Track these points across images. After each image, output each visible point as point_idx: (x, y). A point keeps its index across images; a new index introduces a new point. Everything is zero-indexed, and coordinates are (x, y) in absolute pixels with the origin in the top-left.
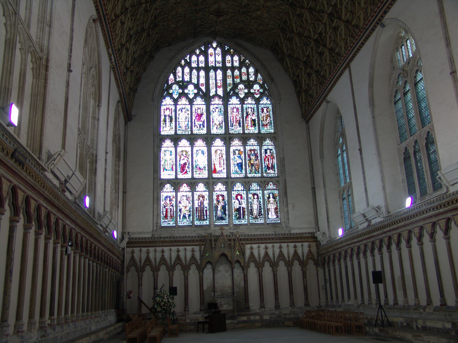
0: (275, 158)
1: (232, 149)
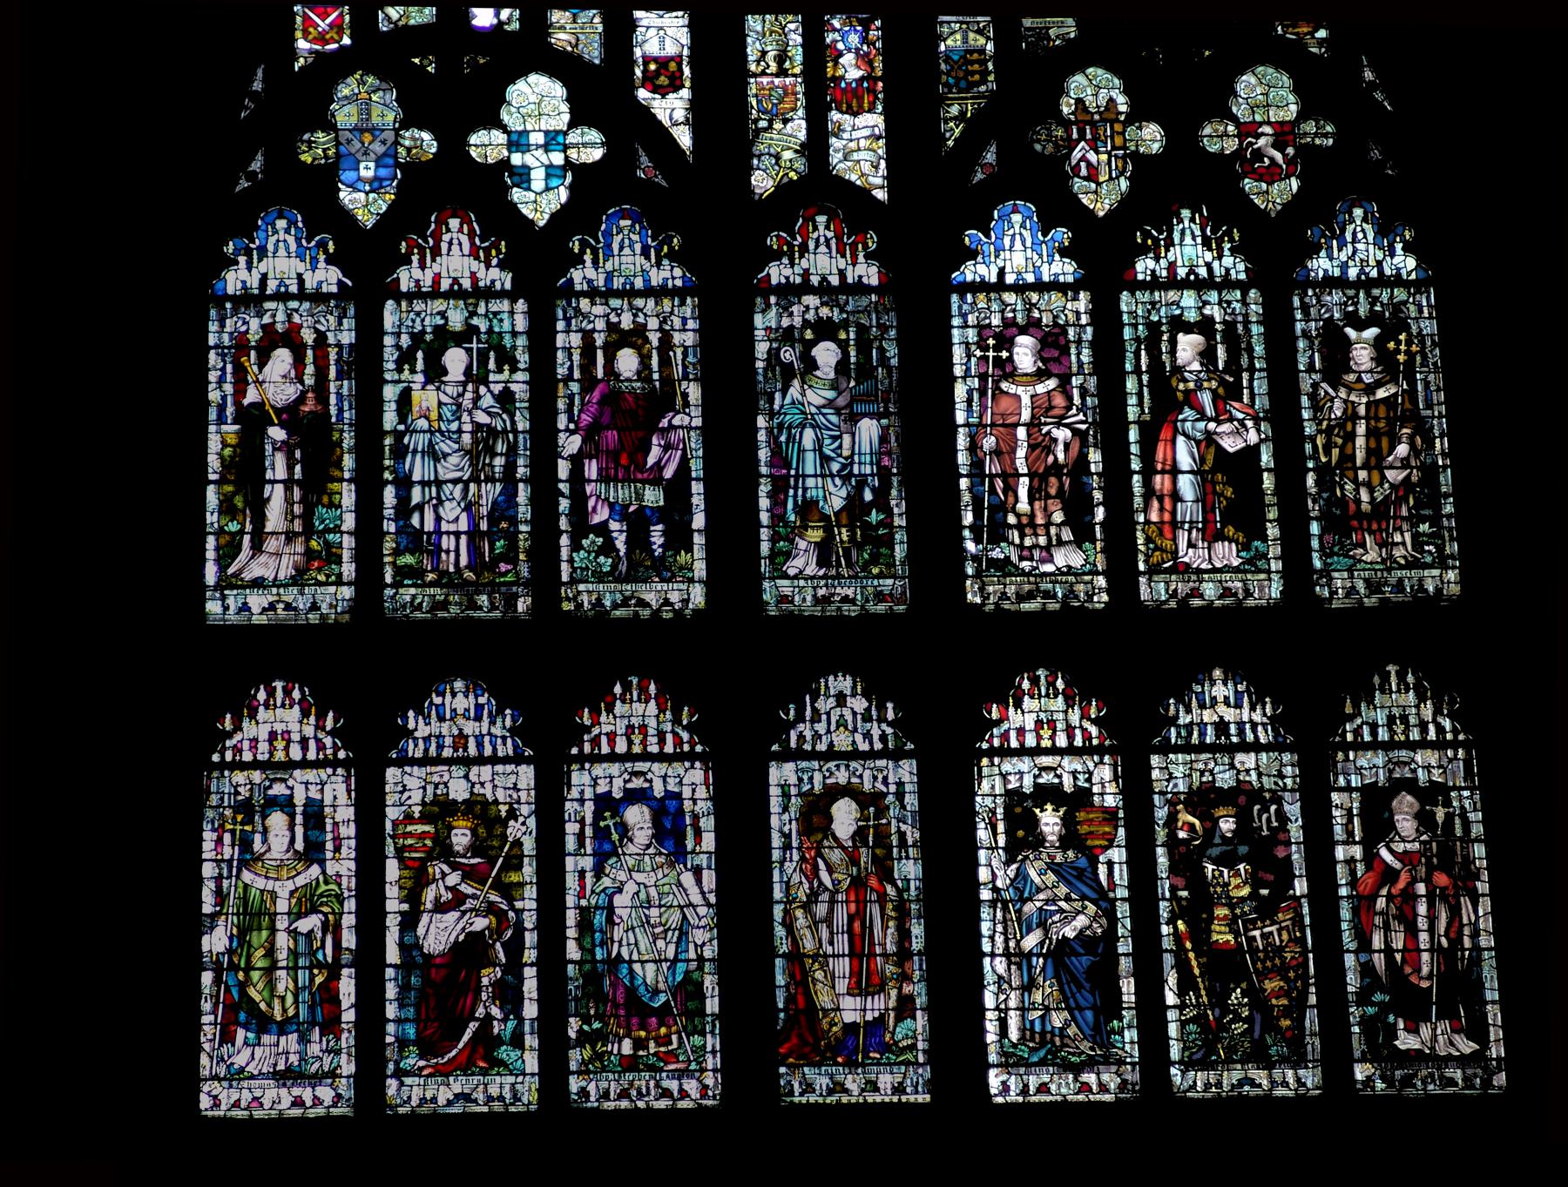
0: (1483, 887)
1: (989, 790)
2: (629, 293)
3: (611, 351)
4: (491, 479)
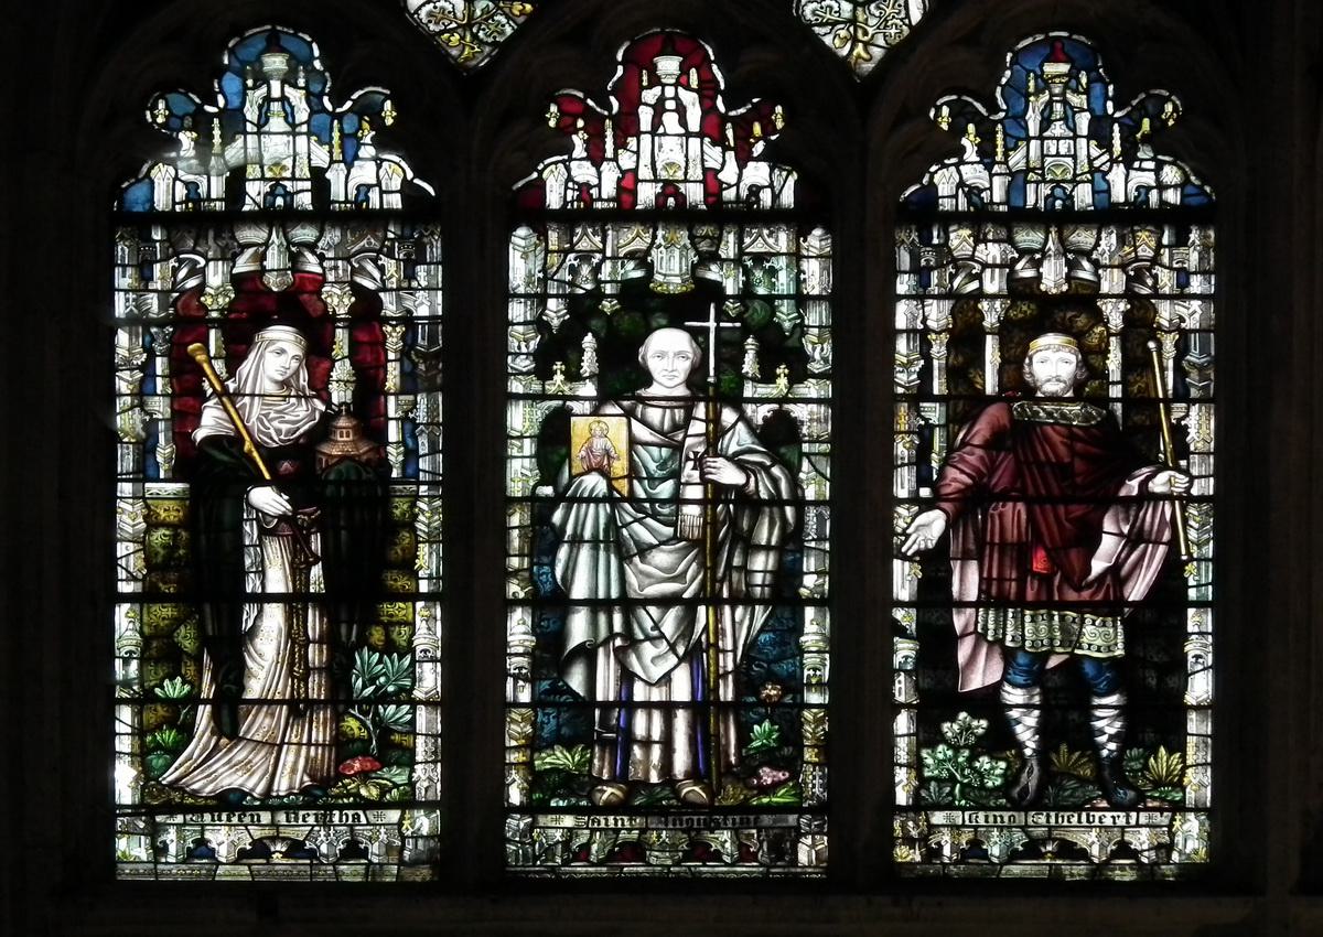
2: (1061, 217)
3: (1018, 339)
4: (744, 599)
